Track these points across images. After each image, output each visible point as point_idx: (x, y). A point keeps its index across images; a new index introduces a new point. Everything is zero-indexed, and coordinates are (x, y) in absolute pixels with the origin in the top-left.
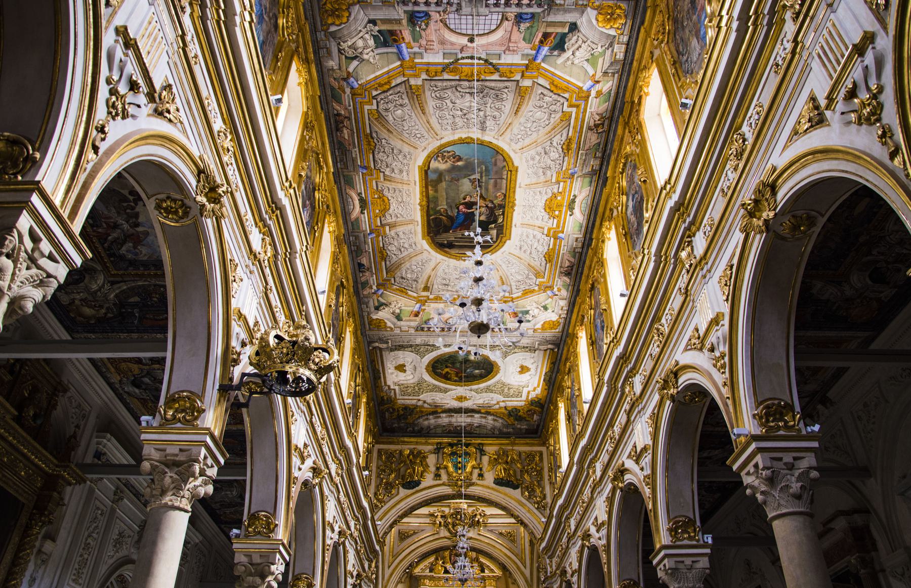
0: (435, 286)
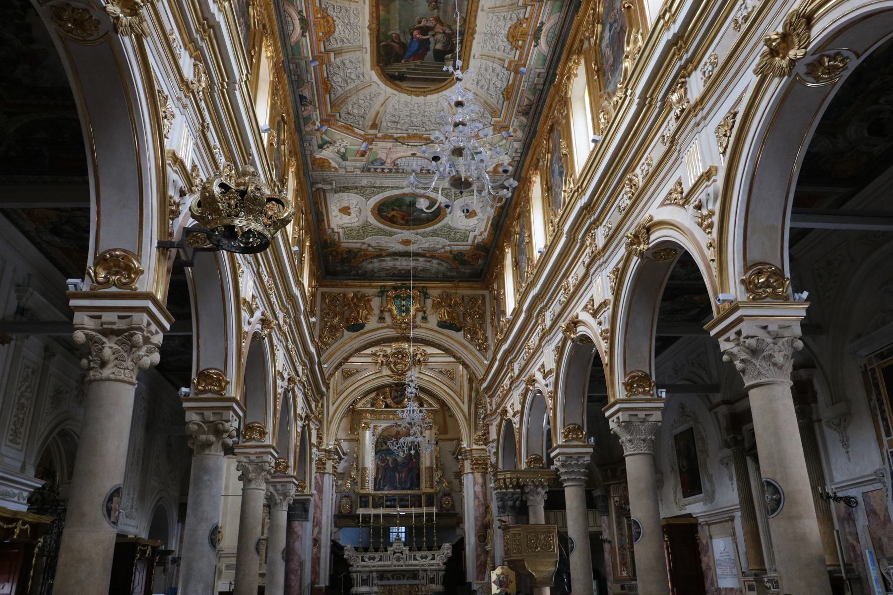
0: (384, 124)
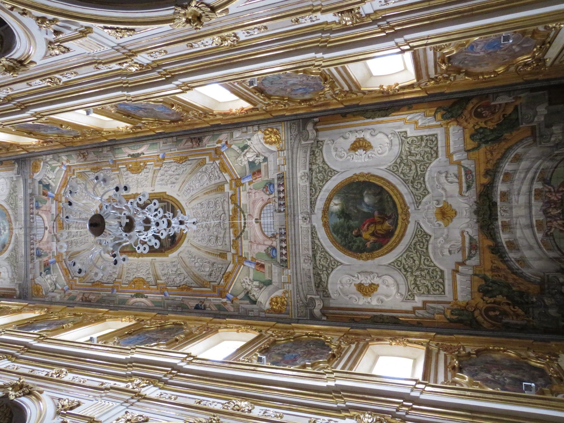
0: (220, 248)
